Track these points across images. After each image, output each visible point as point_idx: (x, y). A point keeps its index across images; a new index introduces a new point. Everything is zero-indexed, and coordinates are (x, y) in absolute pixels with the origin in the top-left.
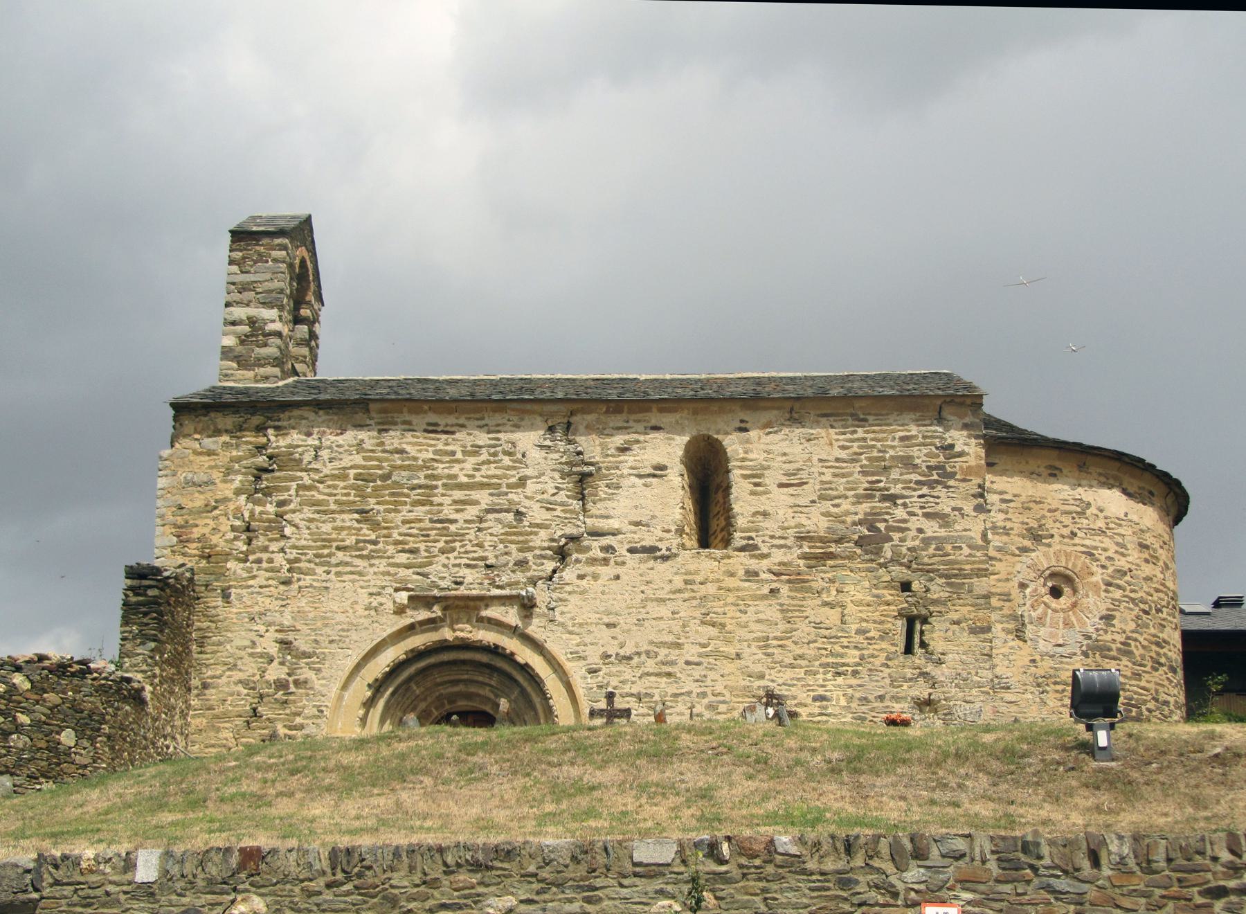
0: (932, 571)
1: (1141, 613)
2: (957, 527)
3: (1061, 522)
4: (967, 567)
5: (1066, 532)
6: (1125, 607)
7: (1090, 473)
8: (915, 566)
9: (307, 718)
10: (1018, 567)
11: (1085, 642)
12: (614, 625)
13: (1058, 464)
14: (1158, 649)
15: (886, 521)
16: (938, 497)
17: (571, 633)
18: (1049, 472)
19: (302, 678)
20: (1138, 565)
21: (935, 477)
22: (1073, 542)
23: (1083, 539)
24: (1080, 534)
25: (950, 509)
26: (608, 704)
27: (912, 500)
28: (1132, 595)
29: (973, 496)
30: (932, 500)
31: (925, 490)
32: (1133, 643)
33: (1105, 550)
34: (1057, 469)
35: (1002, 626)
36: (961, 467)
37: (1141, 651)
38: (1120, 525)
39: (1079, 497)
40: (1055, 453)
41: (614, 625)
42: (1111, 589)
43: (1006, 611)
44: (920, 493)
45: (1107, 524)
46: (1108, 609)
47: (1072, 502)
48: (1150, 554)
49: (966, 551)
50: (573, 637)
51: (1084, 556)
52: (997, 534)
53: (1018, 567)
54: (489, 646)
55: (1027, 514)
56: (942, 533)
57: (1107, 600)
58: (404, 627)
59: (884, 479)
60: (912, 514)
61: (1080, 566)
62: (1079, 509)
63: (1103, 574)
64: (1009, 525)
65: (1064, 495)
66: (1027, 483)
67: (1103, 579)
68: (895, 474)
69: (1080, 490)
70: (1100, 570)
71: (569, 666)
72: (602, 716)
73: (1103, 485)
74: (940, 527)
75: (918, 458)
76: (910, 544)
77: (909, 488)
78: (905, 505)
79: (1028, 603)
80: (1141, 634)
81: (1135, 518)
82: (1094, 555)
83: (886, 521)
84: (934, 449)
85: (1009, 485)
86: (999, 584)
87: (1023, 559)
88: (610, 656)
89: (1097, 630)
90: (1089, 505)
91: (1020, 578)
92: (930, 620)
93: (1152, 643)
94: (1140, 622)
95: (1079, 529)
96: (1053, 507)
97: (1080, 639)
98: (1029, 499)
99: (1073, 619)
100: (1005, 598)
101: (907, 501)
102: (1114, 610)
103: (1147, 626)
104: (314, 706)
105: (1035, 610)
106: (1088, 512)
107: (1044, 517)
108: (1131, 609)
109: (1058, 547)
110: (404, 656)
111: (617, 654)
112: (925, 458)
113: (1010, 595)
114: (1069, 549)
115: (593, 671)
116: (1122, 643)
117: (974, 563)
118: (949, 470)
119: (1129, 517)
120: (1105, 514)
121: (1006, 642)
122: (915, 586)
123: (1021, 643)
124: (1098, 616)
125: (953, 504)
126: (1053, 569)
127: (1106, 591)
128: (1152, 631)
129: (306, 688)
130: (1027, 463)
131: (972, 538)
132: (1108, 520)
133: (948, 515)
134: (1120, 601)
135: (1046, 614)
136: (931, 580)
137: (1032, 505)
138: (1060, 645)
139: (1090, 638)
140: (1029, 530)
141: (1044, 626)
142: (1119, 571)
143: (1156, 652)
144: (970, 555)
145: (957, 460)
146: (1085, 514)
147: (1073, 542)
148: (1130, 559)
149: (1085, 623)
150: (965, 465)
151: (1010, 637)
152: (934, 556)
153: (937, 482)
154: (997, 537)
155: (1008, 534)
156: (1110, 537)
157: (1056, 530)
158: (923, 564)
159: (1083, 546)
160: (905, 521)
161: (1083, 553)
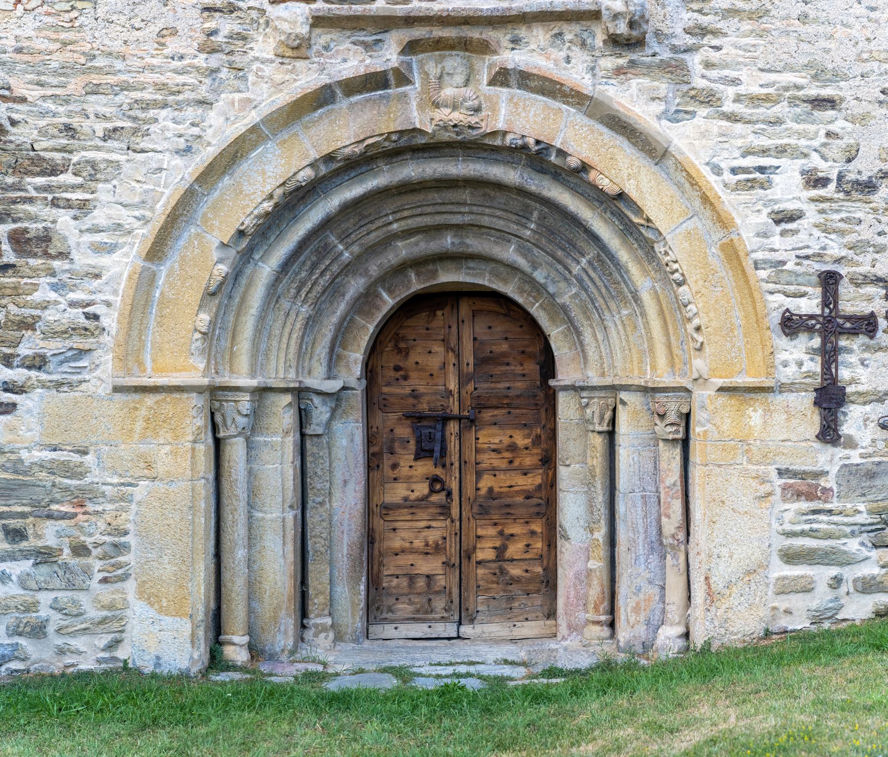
9: (56, 334)
12: (830, 103)
17: (733, 118)
19: (35, 228)
26: (825, 304)
41: (830, 103)
50: (739, 127)
54: (525, 147)
58: (305, 97)
71: (729, 200)
72: (810, 330)
88: (823, 182)
104: (73, 304)
110: (309, 173)
111: (840, 177)
115: (784, 218)
129: (46, 255)
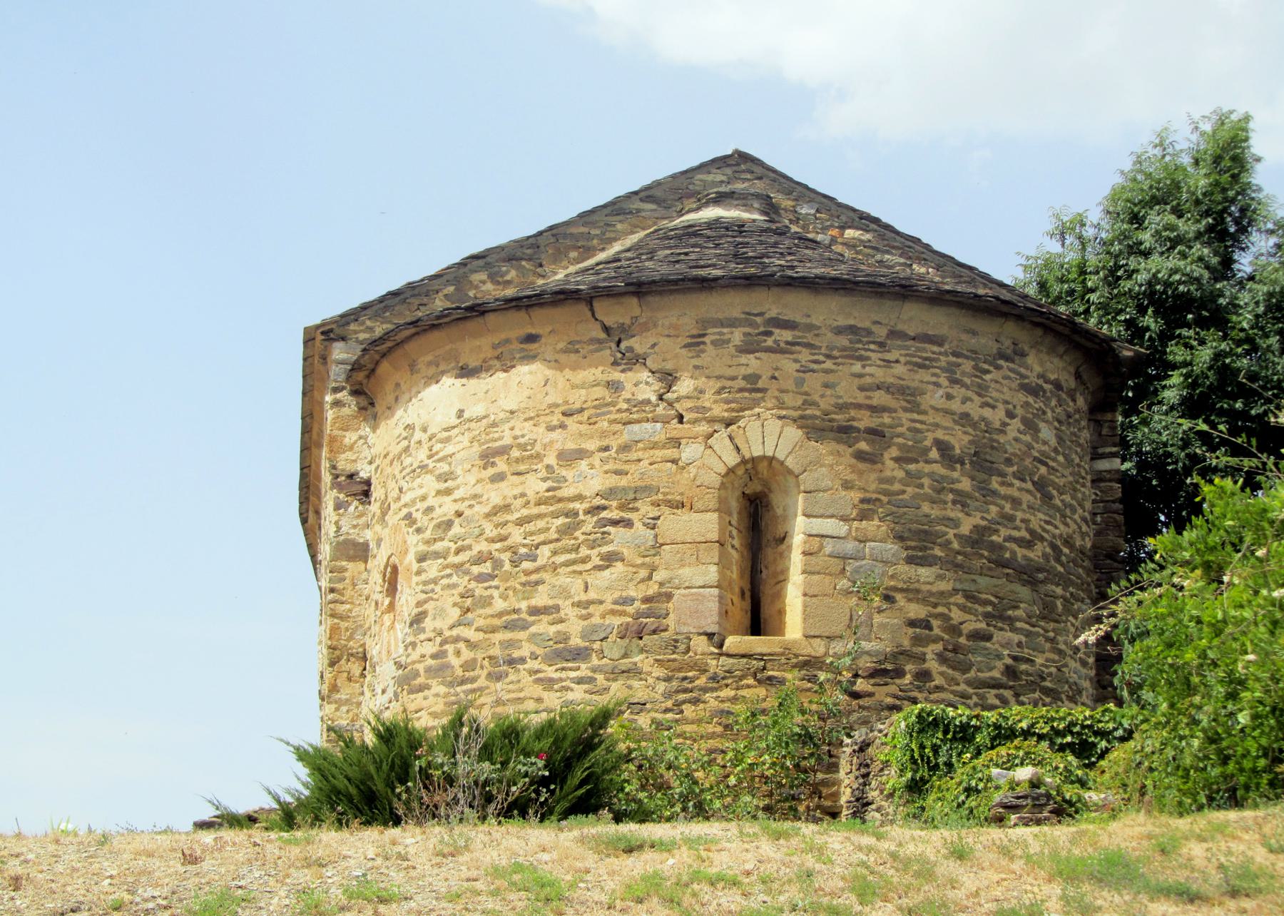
1: (473, 584)
14: (508, 635)
20: (475, 496)
37: (467, 654)
38: (448, 440)
73: (427, 385)
80: (469, 624)
93: (494, 630)
94: (469, 601)
102: (426, 602)
103: (487, 602)
108: (454, 586)
119: (466, 415)
120: (429, 433)
128: (499, 605)
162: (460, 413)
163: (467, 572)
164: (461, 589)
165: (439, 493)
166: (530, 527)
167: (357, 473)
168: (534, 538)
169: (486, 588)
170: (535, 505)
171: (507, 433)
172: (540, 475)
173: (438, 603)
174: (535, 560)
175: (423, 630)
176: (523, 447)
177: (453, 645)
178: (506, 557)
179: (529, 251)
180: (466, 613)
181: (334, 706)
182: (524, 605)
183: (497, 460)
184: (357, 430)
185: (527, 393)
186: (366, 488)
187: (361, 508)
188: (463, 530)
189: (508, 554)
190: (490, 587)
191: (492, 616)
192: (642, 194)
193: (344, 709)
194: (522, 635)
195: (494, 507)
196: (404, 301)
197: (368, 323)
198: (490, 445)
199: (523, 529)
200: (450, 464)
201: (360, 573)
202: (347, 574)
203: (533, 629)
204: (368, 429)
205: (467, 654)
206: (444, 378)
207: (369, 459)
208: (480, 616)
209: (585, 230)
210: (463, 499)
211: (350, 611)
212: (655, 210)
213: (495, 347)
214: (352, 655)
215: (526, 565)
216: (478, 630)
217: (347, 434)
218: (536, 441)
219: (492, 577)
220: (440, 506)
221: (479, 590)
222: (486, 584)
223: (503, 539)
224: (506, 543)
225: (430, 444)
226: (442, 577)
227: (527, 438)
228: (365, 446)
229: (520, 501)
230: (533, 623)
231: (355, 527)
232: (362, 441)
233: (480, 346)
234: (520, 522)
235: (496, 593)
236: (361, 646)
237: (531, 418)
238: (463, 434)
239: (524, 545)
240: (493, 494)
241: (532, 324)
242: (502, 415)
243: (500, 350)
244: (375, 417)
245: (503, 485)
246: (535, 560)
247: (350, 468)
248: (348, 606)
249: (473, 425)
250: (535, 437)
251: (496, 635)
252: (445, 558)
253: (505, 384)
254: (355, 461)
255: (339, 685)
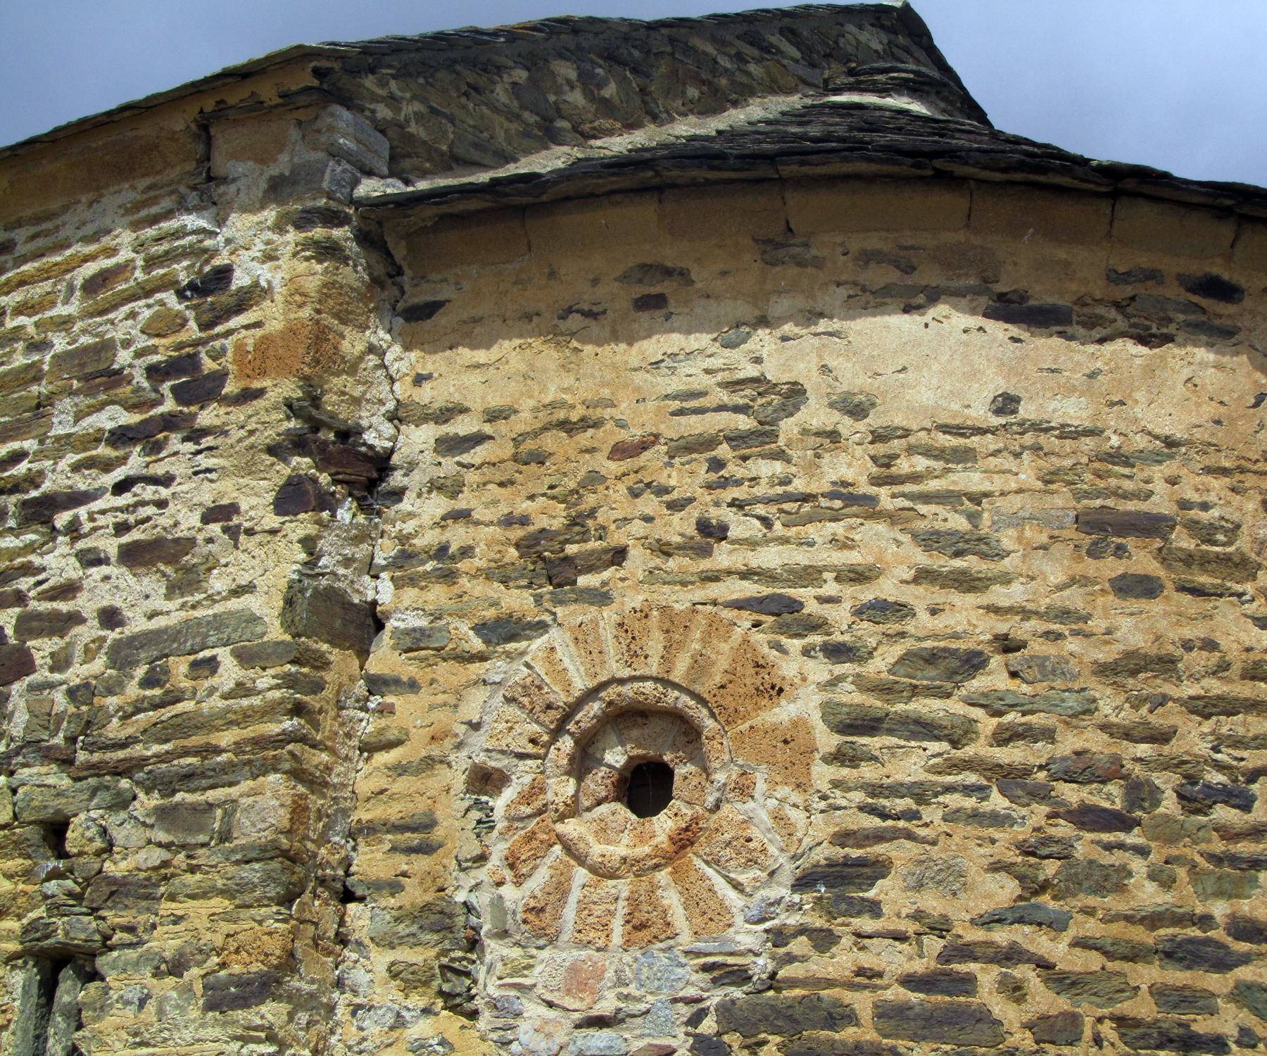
0: (120, 771)
1: (1063, 829)
2: (218, 583)
3: (663, 490)
4: (226, 738)
5: (680, 527)
6: (952, 816)
7: (818, 263)
8: (82, 756)
10: (472, 708)
11: (715, 998)
13: (670, 254)
14: (1178, 976)
15: (20, 598)
16: (167, 480)
18: (640, 290)
20: (1065, 615)
21: (169, 405)
22: (705, 564)
23: (752, 544)
24: (741, 526)
25: (195, 519)
27: (96, 505)
28: (1012, 754)
29: (272, 450)
30: (149, 492)
31: (136, 462)
32: (987, 976)
33: (858, 576)
34: (668, 272)
35: (390, 956)
36: (240, 347)
37: (1043, 999)
38: (965, 456)
39: (751, 371)
40: (645, 212)
42: (872, 743)
43: (413, 895)
44: (119, 474)
45: (887, 461)
46: (843, 837)
47: (724, 397)
48: (1164, 556)
49: (230, 672)
51: (745, 620)
52: (412, 581)
53: (472, 708)
55: (532, 476)
56: (174, 614)
57: (839, 798)
59: (30, 444)
60: (91, 559)
61: (723, 663)
62: (744, 423)
63: (834, 682)
64: (457, 536)
65: (691, 375)
66: (547, 356)
67: (828, 710)
68: (61, 424)
69: (763, 340)
70: (820, 670)
74: (173, 590)
75: (127, 344)
76: (76, 673)
77: (90, 463)
78: (74, 530)
79: (498, 851)
80: (1056, 925)
81: (1073, 411)
82: (794, 606)
83: (20, 598)
84: (170, 298)
85: (475, 378)
86: (401, 785)
87: (496, 669)
89: (779, 937)
90: (795, 394)
91: (478, 750)
92: (102, 962)
93: (1135, 954)
94: (1050, 868)
95: (736, 504)
96: (634, 433)
97: (693, 982)
98: (544, 417)
99: (672, 899)
100: (414, 839)
101: (82, 512)
102: (879, 837)
103: (1114, 880)
105: (519, 880)
106: (788, 427)
107: (594, 479)
108: (997, 820)
109: (636, 600)
112: (143, 342)
113: (428, 824)
114: (681, 600)
116: (910, 981)
117: (246, 717)
118: (208, 365)
119: (1027, 411)
120: (874, 420)
121: (399, 1022)
122: (73, 838)
123: (450, 1023)
124: (788, 872)
125: (207, 495)
126: (611, 693)
127: (839, 757)
128: (1148, 895)
130: (552, 275)
131: (254, 619)
132: (896, 445)
133: (188, 544)
134: (921, 793)
135: (560, 889)
136: (122, 802)
137: (552, 441)
138: (600, 1022)
139: (740, 976)
140: (525, 546)
141: (553, 940)
142: (931, 658)
143: (1160, 993)
144: (241, 690)
145: (236, 322)
146: (774, 436)
147: (705, 564)
148: (1013, 594)
149: (724, 909)
150: (250, 338)
151: (417, 1001)
152: (138, 707)
153: (170, 423)
154: (410, 594)
155: (448, 577)
156: (892, 518)
157: (638, 528)
158: (105, 747)
159: (746, 574)
160: (69, 590)
161: (739, 605)
162: (1006, 404)
163: (1040, 794)
164: (1022, 832)
165: (924, 576)
166: (1227, 725)
167: (359, 431)
168: (1245, 754)
169: (1109, 847)
170: (1243, 677)
171: (1159, 486)
172: (1250, 608)
173: (934, 852)
174: (1246, 807)
175: (874, 909)
176: (1206, 533)
177: (995, 971)
178: (1167, 782)
179: (636, 53)
180: (1036, 893)
181: (284, 1008)
182: (1220, 909)
183: (1130, 542)
184: (363, 328)
185: (1210, 410)
186: (375, 475)
187: (361, 519)
188: (1025, 688)
189: (1176, 779)
190: (1121, 846)
191: (1129, 919)
192: (787, 21)
193: (303, 1017)
194: (1214, 982)
195: (1129, 655)
196: (450, 65)
197: (393, 85)
198: (1110, 503)
199: (1207, 727)
200: (973, 517)
201: (352, 679)
202: (329, 676)
203: (1244, 973)
204: (381, 333)
205: (1043, 999)
206: (941, 309)
207: (391, 405)
208: (1089, 912)
209: (710, 49)
210: (1026, 614)
211: (328, 769)
212: (797, 61)
213: (1115, 277)
214: (322, 882)
215: (1223, 813)
216: (1081, 943)
217: (347, 331)
218: (1238, 527)
219: (1122, 822)
220: (934, 612)
221: (1085, 845)
222: (1106, 837)
223: (1162, 737)
224: (1166, 749)
225: (881, 449)
226: (949, 789)
227: (1215, 513)
228: (380, 373)
229: (1199, 660)
230: (1245, 959)
231: (347, 562)
232: (372, 360)
233: (1067, 264)
234: (1203, 708)
235: (1138, 865)
236: (340, 862)
237: (1225, 472)
238: (1017, 455)
239: (1220, 767)
240: (1126, 623)
241: (1229, 258)
242: (1141, 442)
243: (1129, 291)
244: (425, 311)
245: (1155, 607)
246: (1246, 807)
247: (344, 412)
248: (325, 757)
249: (1050, 441)
250: (1236, 517)
251: (1139, 967)
252: (955, 744)
253: (1149, 371)
254: (356, 401)
255: (299, 955)
